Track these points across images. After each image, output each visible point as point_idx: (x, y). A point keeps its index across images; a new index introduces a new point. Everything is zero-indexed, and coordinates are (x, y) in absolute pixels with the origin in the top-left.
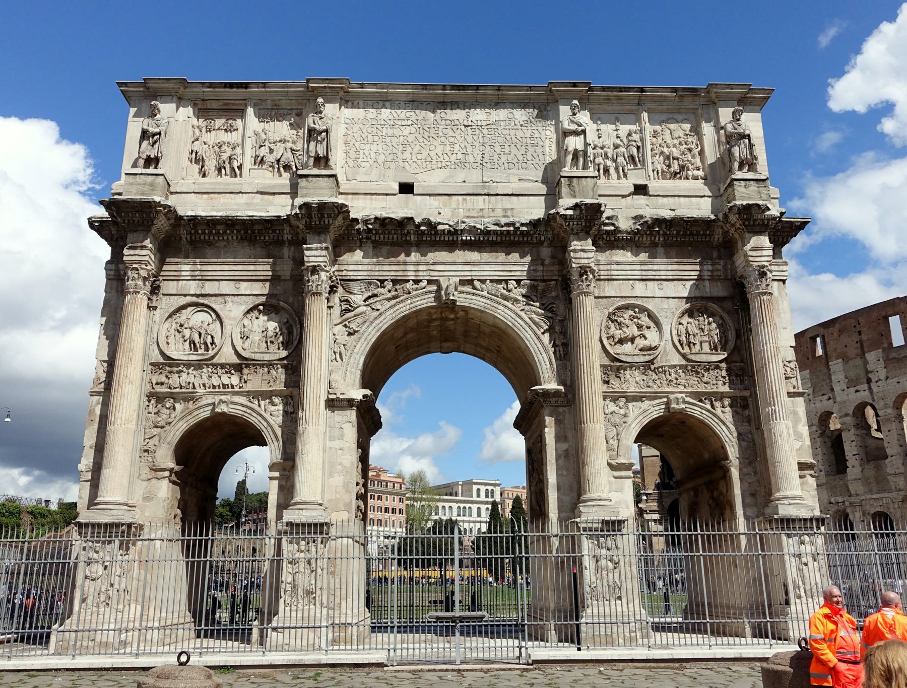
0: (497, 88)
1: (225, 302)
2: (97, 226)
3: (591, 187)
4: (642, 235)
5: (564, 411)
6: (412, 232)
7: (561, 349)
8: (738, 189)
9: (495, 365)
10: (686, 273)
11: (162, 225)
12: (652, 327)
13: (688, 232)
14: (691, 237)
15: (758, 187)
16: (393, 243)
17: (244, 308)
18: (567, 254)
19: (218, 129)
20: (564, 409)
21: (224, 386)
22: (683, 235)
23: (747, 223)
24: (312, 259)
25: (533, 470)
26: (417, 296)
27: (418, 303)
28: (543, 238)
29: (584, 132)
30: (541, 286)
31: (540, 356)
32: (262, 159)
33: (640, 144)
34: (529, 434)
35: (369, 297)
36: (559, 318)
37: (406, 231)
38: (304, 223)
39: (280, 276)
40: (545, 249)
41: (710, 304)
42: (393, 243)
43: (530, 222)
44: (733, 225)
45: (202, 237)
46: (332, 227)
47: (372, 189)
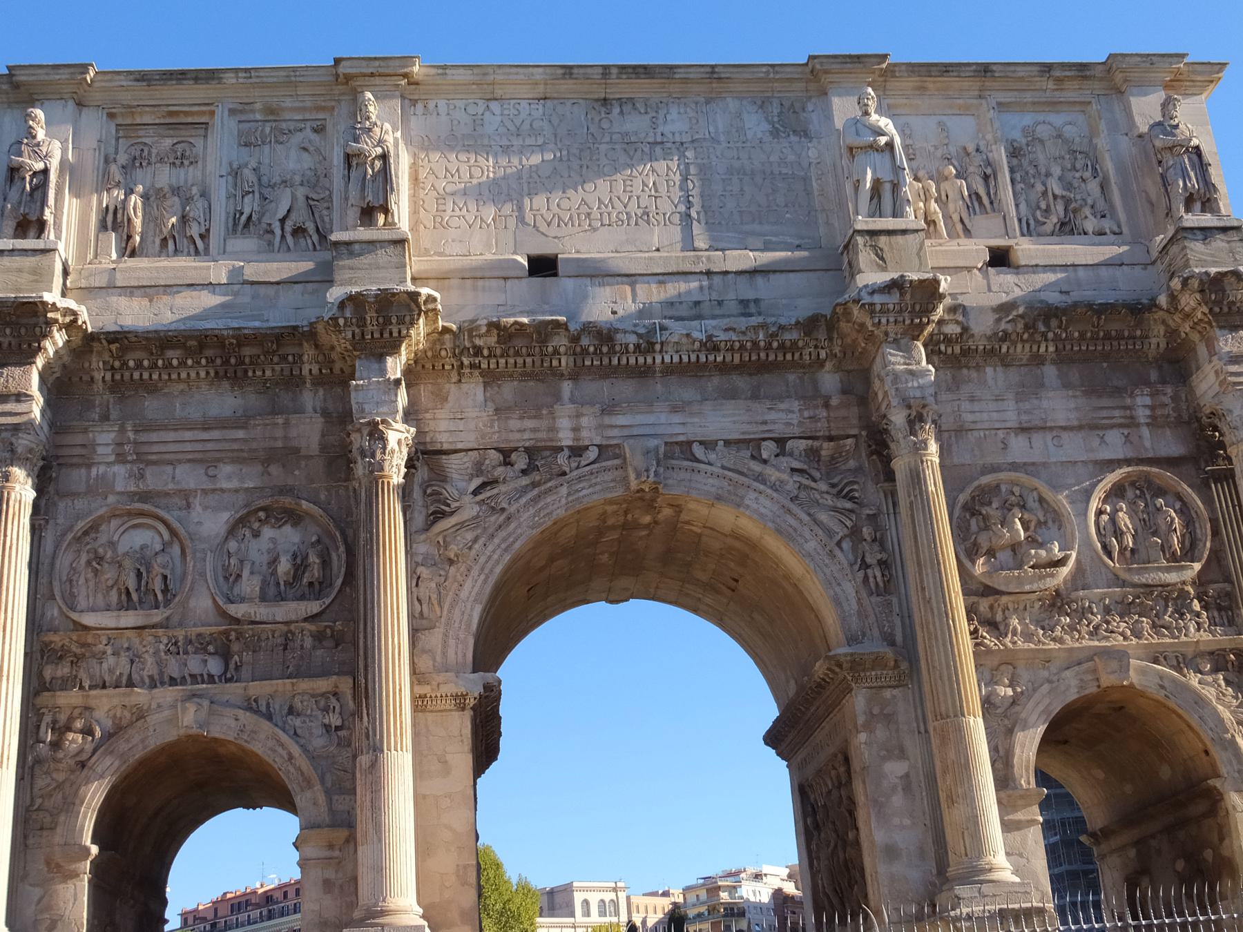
0: (709, 70)
1: (188, 506)
3: (915, 251)
4: (1014, 343)
5: (894, 697)
6: (562, 350)
7: (878, 574)
9: (719, 619)
10: (1104, 413)
12: (1050, 523)
13: (1102, 334)
14: (1107, 343)
15: (1229, 242)
16: (524, 374)
17: (225, 516)
19: (161, 161)
20: (895, 692)
22: (1092, 338)
23: (1217, 310)
25: (817, 827)
26: (580, 479)
27: (585, 492)
28: (823, 354)
30: (827, 449)
33: (989, 171)
34: (800, 756)
35: (484, 485)
37: (550, 349)
38: (350, 335)
39: (297, 451)
42: (524, 374)
43: (798, 323)
44: (1187, 316)
45: (136, 375)
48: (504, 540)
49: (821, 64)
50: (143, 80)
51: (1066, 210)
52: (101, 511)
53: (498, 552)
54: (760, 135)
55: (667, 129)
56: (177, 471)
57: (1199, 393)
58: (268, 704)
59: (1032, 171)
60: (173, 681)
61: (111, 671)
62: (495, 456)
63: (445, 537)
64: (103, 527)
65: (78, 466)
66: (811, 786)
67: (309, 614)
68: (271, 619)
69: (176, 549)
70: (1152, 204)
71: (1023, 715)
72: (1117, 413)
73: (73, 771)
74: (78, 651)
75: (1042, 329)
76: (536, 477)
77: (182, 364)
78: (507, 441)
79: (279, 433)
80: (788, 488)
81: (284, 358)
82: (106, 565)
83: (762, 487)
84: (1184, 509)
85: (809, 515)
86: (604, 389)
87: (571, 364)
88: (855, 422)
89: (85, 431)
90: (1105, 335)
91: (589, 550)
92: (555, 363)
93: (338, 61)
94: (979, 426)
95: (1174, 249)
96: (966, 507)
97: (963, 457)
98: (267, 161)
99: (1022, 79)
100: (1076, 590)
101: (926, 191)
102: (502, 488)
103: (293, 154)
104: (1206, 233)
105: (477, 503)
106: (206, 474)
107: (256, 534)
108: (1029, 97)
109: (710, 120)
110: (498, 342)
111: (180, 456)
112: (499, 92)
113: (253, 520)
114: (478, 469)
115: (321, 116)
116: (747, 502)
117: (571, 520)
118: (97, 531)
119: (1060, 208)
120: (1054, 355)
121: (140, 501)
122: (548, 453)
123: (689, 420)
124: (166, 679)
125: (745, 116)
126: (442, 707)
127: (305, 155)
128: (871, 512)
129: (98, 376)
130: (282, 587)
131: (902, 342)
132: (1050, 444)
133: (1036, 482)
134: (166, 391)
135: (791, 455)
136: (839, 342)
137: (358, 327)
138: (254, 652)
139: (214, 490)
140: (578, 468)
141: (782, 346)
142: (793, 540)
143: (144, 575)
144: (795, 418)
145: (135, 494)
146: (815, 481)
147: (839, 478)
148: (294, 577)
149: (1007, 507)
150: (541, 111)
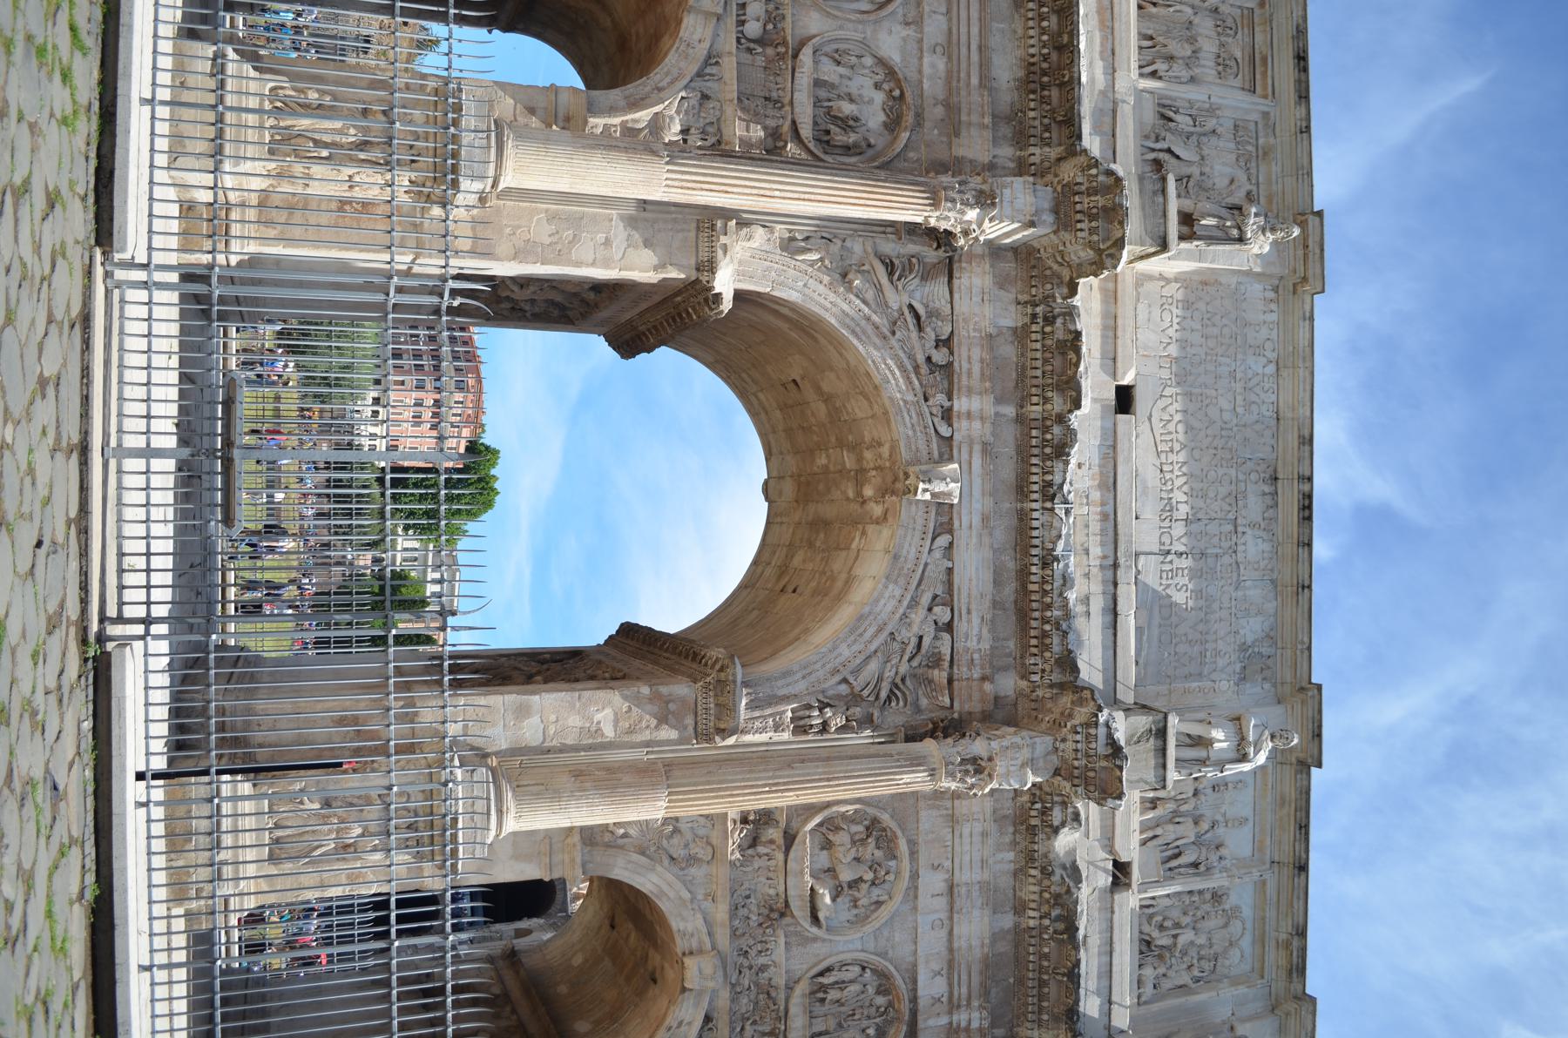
1: (907, 24)
4: (1039, 883)
5: (685, 728)
6: (1049, 407)
9: (745, 585)
10: (964, 977)
12: (855, 911)
13: (1046, 977)
14: (1036, 983)
16: (1024, 368)
17: (896, 58)
18: (1012, 730)
19: (1222, 45)
20: (691, 729)
22: (1041, 967)
24: (1007, 192)
25: (543, 662)
26: (920, 415)
29: (1244, 758)
30: (940, 676)
31: (799, 675)
32: (1170, 120)
33: (1202, 868)
35: (917, 317)
36: (876, 714)
37: (1050, 394)
38: (1079, 180)
39: (957, 135)
40: (1012, 683)
41: (905, 1028)
42: (1024, 368)
43: (1070, 652)
46: (1066, 236)
47: (1124, 330)
48: (864, 332)
49: (1313, 697)
50: (1298, 31)
51: (1163, 947)
53: (852, 324)
55: (1249, 538)
56: (941, 17)
59: (1199, 914)
66: (582, 659)
68: (796, 87)
71: (659, 868)
72: (964, 990)
75: (1055, 912)
76: (924, 369)
77: (1043, 31)
78: (960, 344)
79: (975, 118)
80: (904, 631)
81: (1047, 129)
83: (905, 603)
85: (876, 652)
86: (1008, 449)
87: (1033, 416)
88: (967, 707)
90: (1044, 981)
91: (833, 439)
92: (1035, 400)
93: (1320, 214)
94: (957, 840)
96: (875, 821)
97: (928, 820)
98: (1221, 144)
100: (786, 936)
101: (1185, 801)
102: (914, 334)
103: (1228, 170)
105: (901, 309)
106: (937, 44)
107: (877, 86)
108: (1271, 914)
110: (1058, 341)
112: (1284, 373)
113: (892, 85)
114: (933, 314)
115: (1262, 199)
116: (891, 587)
117: (876, 407)
119: (1164, 941)
120: (1024, 926)
122: (946, 386)
123: (974, 532)
125: (1260, 618)
127: (1227, 181)
128: (875, 718)
130: (826, 104)
131: (1055, 757)
132: (936, 916)
133: (898, 898)
134: (1016, 16)
135: (936, 638)
136: (1047, 695)
137: (1087, 189)
138: (765, 68)
139: (921, 50)
140: (931, 414)
141: (1045, 635)
142: (852, 632)
144: (972, 644)
146: (909, 661)
148: (835, 117)
149: (874, 866)
150: (1267, 414)
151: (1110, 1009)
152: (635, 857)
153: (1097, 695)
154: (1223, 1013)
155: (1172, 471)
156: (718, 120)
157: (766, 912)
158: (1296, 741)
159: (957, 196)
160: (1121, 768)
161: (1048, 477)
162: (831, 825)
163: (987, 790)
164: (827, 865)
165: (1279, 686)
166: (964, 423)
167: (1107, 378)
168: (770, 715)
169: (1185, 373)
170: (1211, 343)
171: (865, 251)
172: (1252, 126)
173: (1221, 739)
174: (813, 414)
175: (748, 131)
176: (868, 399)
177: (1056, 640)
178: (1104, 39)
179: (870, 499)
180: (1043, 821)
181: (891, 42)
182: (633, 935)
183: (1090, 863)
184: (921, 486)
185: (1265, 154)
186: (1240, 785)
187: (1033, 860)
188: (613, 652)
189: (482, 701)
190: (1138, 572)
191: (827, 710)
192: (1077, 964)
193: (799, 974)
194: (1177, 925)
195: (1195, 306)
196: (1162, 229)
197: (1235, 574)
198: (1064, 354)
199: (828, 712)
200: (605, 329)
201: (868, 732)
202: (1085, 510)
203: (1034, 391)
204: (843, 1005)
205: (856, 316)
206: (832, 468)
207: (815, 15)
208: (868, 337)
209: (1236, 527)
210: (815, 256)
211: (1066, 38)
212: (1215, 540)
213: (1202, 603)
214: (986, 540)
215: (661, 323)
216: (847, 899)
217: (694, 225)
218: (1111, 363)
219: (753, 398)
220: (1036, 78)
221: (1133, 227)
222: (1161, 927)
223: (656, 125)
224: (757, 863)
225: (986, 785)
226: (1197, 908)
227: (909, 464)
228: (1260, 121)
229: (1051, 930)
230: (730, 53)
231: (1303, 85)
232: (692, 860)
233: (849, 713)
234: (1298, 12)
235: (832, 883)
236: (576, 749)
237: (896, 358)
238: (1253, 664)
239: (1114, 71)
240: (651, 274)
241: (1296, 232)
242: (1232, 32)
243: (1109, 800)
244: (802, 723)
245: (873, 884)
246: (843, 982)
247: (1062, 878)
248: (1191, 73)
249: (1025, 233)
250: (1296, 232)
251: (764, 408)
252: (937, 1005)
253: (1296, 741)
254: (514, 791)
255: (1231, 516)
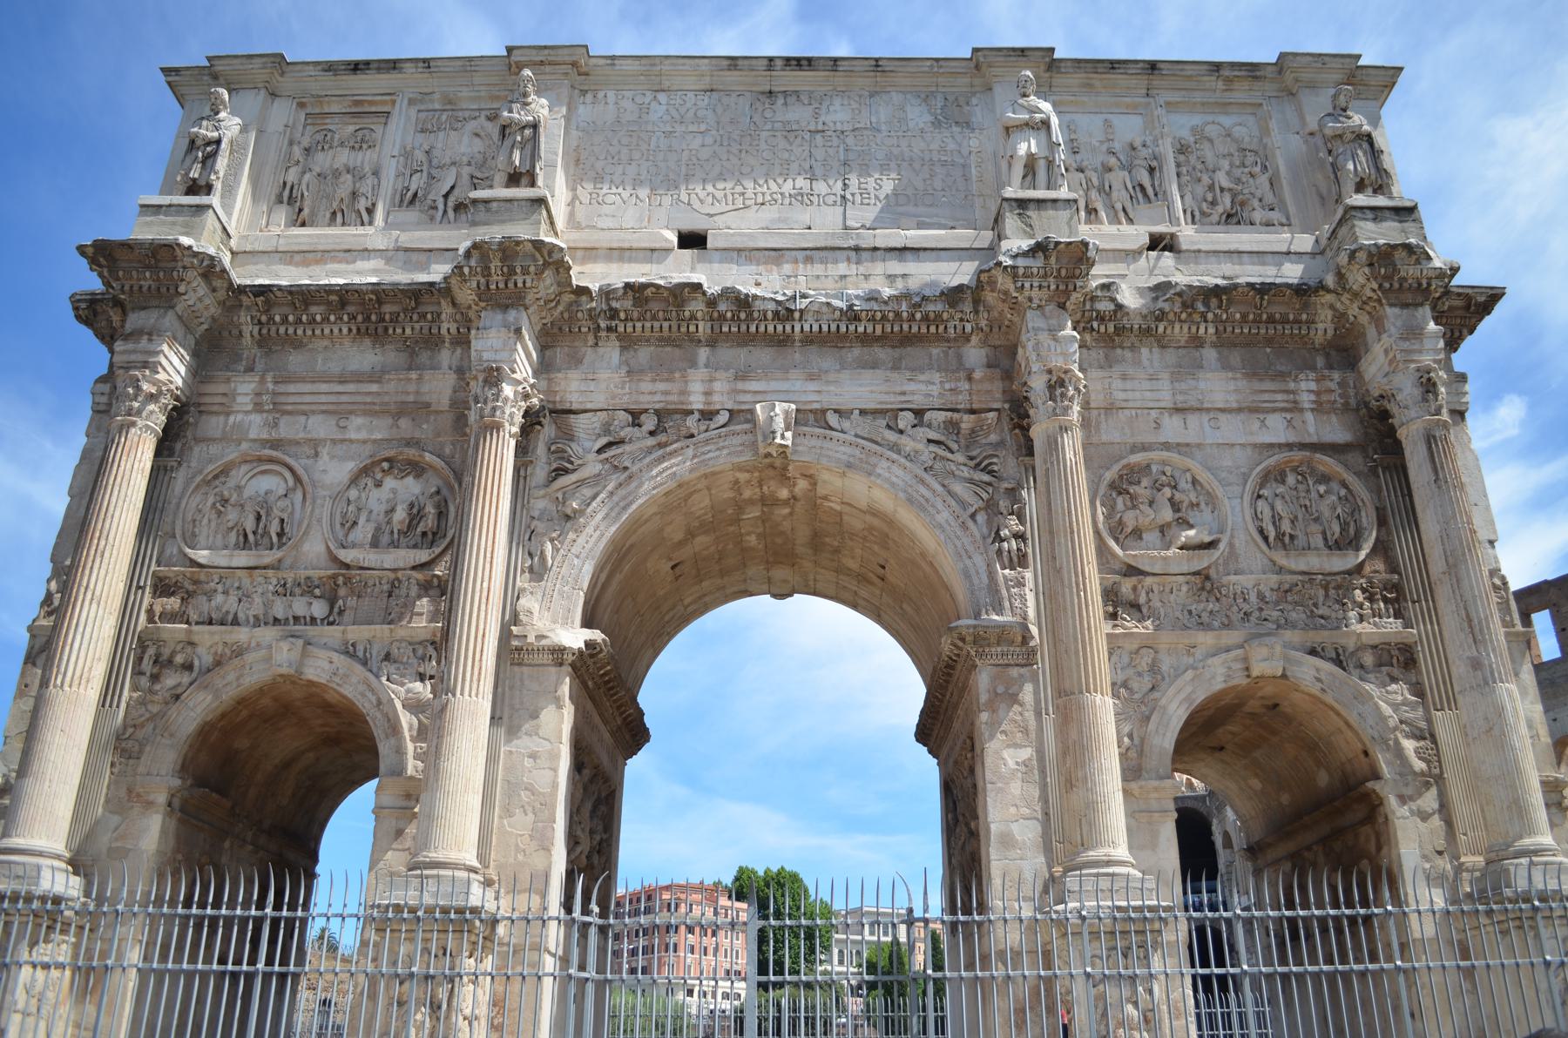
1: (317, 455)
2: (89, 311)
4: (1172, 323)
5: (1021, 676)
6: (699, 315)
8: (1361, 224)
9: (877, 615)
10: (1266, 397)
11: (200, 299)
12: (1203, 505)
13: (1265, 317)
14: (1271, 326)
16: (661, 339)
17: (350, 466)
19: (342, 144)
20: (1023, 670)
21: (296, 619)
22: (1254, 321)
23: (1387, 285)
24: (486, 356)
25: (956, 821)
28: (968, 328)
29: (1046, 124)
30: (967, 422)
32: (415, 195)
33: (1154, 164)
35: (610, 445)
37: (687, 314)
38: (474, 285)
39: (428, 405)
40: (973, 350)
42: (661, 339)
43: (942, 293)
44: (1356, 295)
45: (282, 330)
46: (530, 298)
47: (623, 241)
48: (624, 498)
49: (985, 56)
50: (329, 70)
52: (231, 457)
53: (617, 510)
54: (921, 125)
55: (829, 119)
57: (1367, 377)
58: (365, 652)
59: (1199, 166)
60: (276, 621)
61: (218, 608)
62: (624, 417)
63: (564, 494)
64: (233, 472)
65: (216, 413)
66: (953, 781)
67: (418, 563)
68: (378, 566)
69: (299, 495)
70: (1322, 198)
71: (1163, 702)
72: (1279, 397)
73: (167, 703)
74: (191, 588)
75: (1201, 308)
76: (662, 438)
77: (326, 320)
78: (636, 402)
80: (923, 458)
81: (423, 316)
82: (230, 508)
83: (895, 456)
84: (1349, 497)
85: (944, 486)
86: (741, 355)
88: (998, 395)
89: (228, 380)
91: (731, 529)
92: (692, 328)
93: (510, 50)
94: (1130, 404)
95: (1343, 231)
97: (1112, 432)
98: (440, 145)
99: (1189, 77)
101: (1089, 180)
102: (627, 448)
103: (466, 139)
104: (1377, 213)
106: (338, 425)
107: (378, 485)
108: (1198, 97)
109: (873, 111)
110: (634, 305)
111: (314, 407)
112: (666, 84)
113: (377, 470)
116: (879, 471)
117: (699, 486)
118: (227, 476)
119: (1227, 200)
120: (1214, 338)
121: (271, 448)
122: (678, 416)
123: (824, 388)
124: (271, 620)
125: (908, 108)
126: (536, 662)
127: (477, 140)
128: (1010, 486)
129: (247, 330)
132: (1207, 429)
133: (1189, 463)
135: (929, 426)
138: (359, 597)
139: (343, 441)
140: (706, 431)
141: (926, 318)
142: (924, 510)
143: (264, 518)
145: (267, 441)
147: (979, 450)
149: (1157, 487)
150: (706, 101)
151: (1295, 253)
152: (1152, 726)
153: (985, 267)
154: (1296, 144)
155: (763, 194)
156: (410, 644)
157: (1205, 594)
158: (1028, 73)
159: (490, 405)
160: (1057, 243)
161: (770, 315)
162: (1117, 530)
163: (1081, 375)
164: (1158, 534)
165: (977, 89)
166: (716, 398)
167: (671, 257)
168: (1008, 591)
169: (666, 180)
170: (636, 155)
171: (544, 497)
172: (421, 114)
173: (1026, 146)
174: (707, 548)
175: (422, 614)
176: (691, 494)
177: (931, 307)
178: (334, 260)
179: (791, 492)
180: (1110, 320)
181: (334, 471)
182: (1230, 728)
183: (1151, 273)
184: (778, 441)
185: (450, 103)
186: (1072, 127)
187: (1149, 329)
188: (945, 750)
189: (997, 882)
190: (863, 227)
191: (1002, 533)
192: (1251, 285)
193: (1266, 561)
194: (1211, 188)
195: (600, 171)
196: (523, 203)
197: (865, 132)
198: (647, 300)
199: (1005, 533)
200: (620, 759)
201: (1024, 493)
202: (802, 279)
203: (683, 329)
204: (1296, 517)
205: (610, 505)
206: (760, 530)
207: (306, 547)
208: (629, 494)
209: (818, 132)
210: (549, 546)
211: (333, 298)
212: (831, 151)
213: (893, 165)
214: (832, 377)
215: (615, 701)
216: (1191, 513)
217: (516, 668)
218: (656, 254)
219: (690, 609)
220: (372, 327)
221: (521, 231)
222: (1214, 203)
223: (415, 706)
224: (1156, 603)
225: (1075, 376)
226: (1194, 169)
227: (756, 453)
228: (417, 108)
229: (1218, 311)
230: (344, 632)
231: (383, 65)
232: (1154, 668)
233: (1005, 512)
234: (311, 71)
235: (1174, 529)
236: (1044, 787)
237: (650, 466)
238: (953, 114)
239: (366, 250)
240: (565, 711)
241: (527, 72)
242: (329, 135)
243: (1089, 254)
244: (1015, 559)
245: (1175, 487)
246: (1273, 517)
247: (1166, 300)
248: (369, 174)
249: (527, 337)
250: (527, 72)
251: (700, 598)
252: (1295, 424)
253: (1028, 73)
254: (1087, 849)
255: (807, 136)
